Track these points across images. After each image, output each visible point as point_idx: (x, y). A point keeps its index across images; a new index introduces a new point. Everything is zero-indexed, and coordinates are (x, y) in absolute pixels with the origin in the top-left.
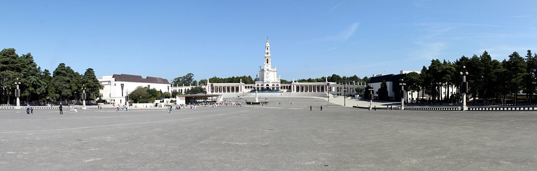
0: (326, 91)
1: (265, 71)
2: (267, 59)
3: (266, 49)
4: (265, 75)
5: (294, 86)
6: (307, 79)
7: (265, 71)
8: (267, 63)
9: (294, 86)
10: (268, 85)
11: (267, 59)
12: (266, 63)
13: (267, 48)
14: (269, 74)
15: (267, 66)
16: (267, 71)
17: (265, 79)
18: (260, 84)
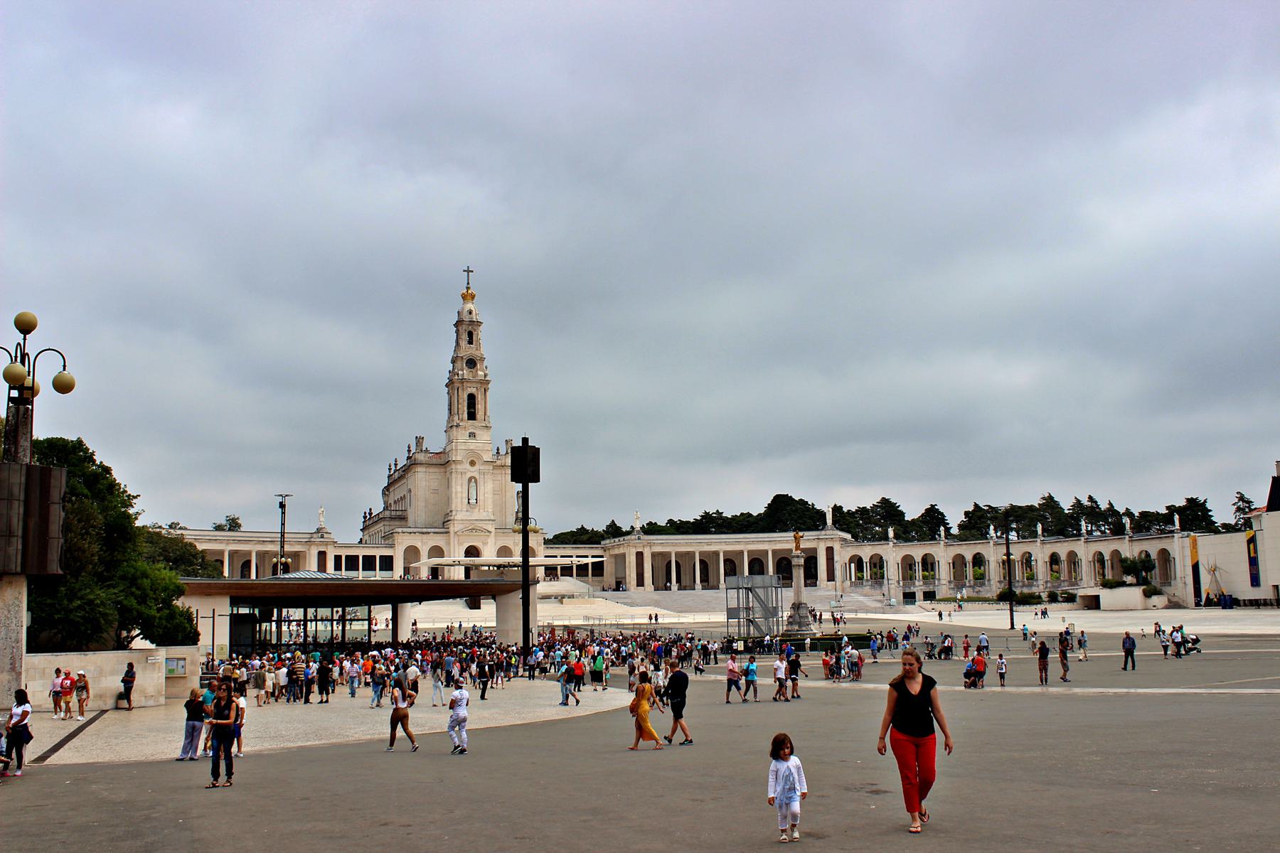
0: (831, 577)
1: (460, 462)
2: (472, 398)
3: (465, 337)
4: (459, 490)
5: (640, 555)
6: (692, 515)
7: (460, 462)
8: (472, 416)
9: (640, 555)
10: (472, 552)
11: (472, 398)
12: (466, 416)
13: (470, 334)
14: (480, 482)
15: (472, 435)
16: (472, 463)
17: (461, 515)
18: (424, 547)
